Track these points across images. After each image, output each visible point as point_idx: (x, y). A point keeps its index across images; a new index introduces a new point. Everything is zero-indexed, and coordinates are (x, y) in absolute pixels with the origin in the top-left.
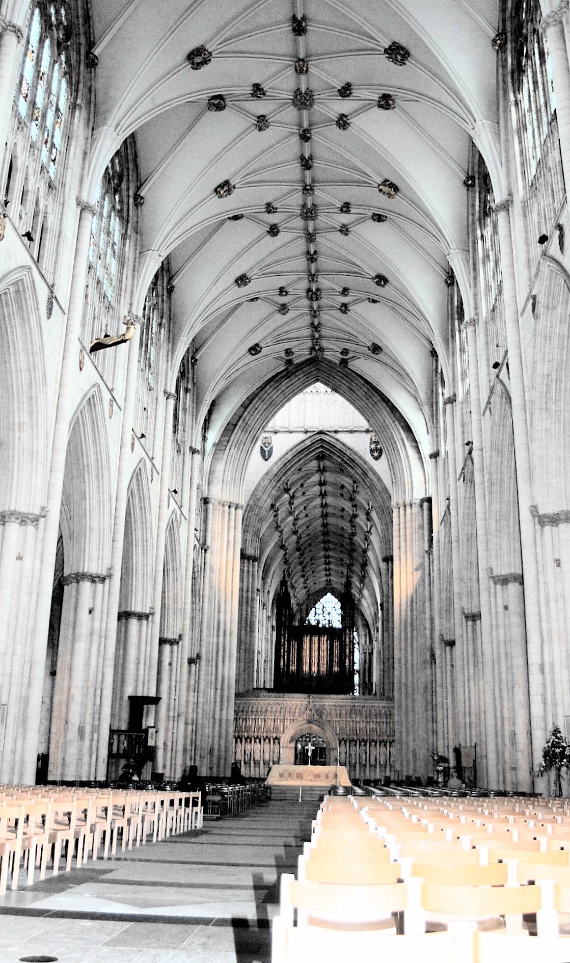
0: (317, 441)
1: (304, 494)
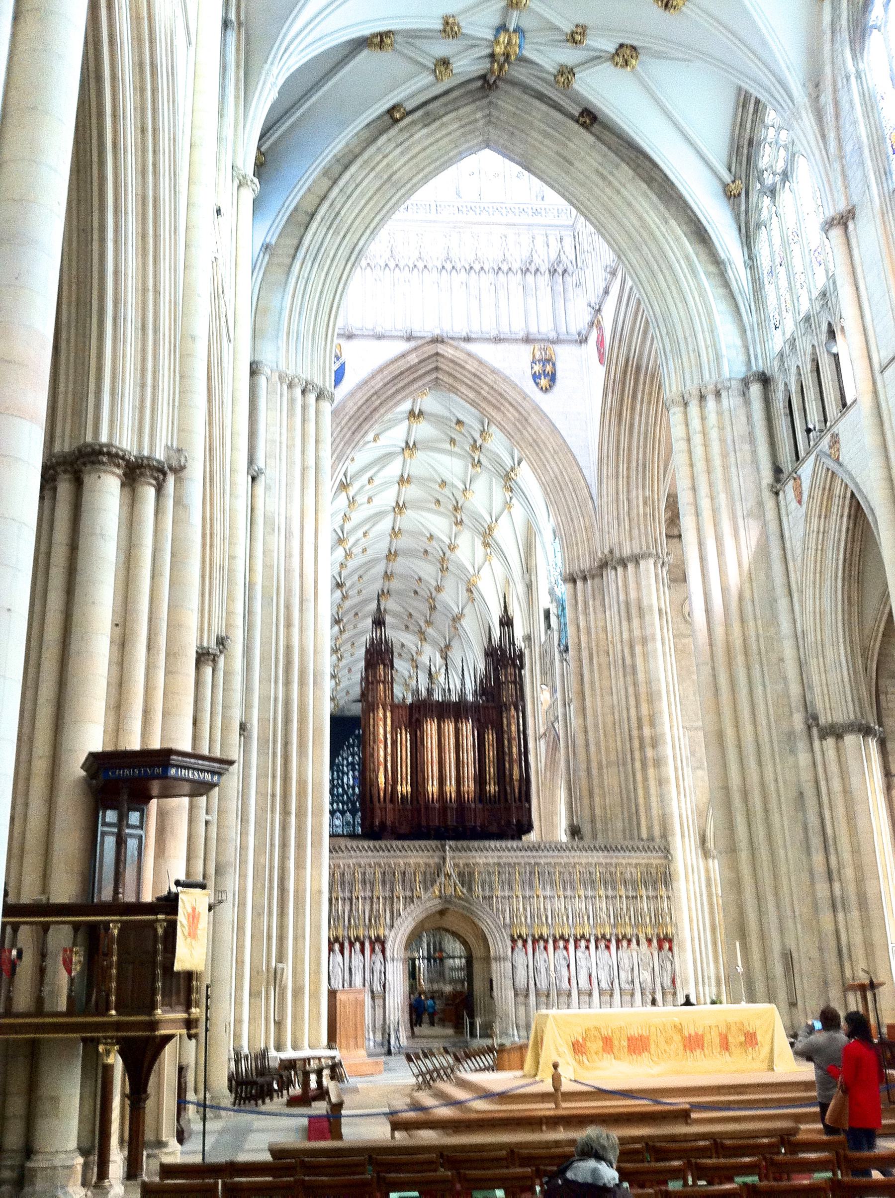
0: (429, 357)
1: (370, 500)
